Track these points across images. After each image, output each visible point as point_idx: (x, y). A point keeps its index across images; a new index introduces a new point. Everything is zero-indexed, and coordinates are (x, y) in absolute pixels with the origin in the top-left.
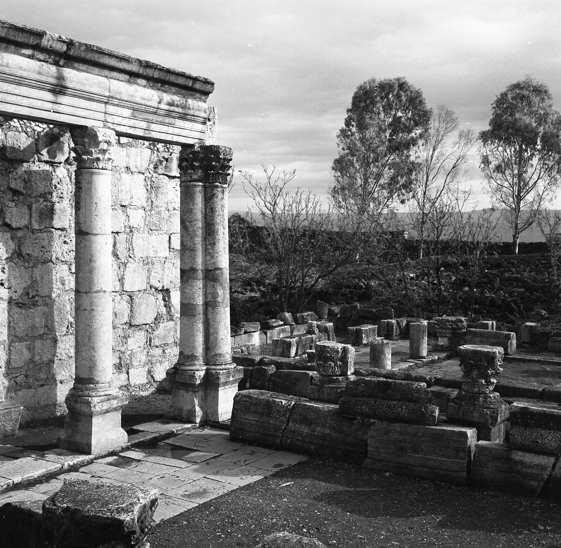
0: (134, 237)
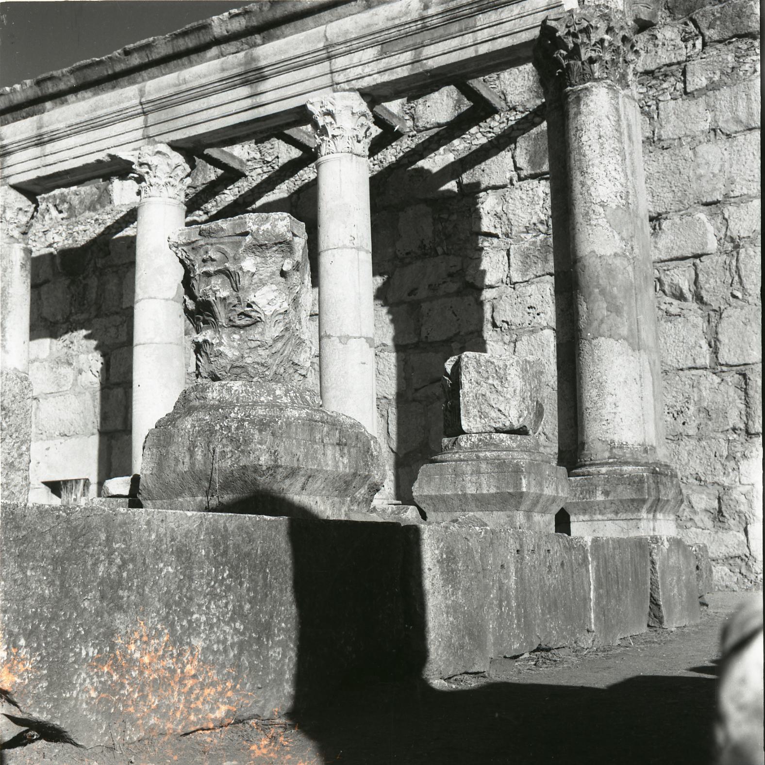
0: (742, 256)
